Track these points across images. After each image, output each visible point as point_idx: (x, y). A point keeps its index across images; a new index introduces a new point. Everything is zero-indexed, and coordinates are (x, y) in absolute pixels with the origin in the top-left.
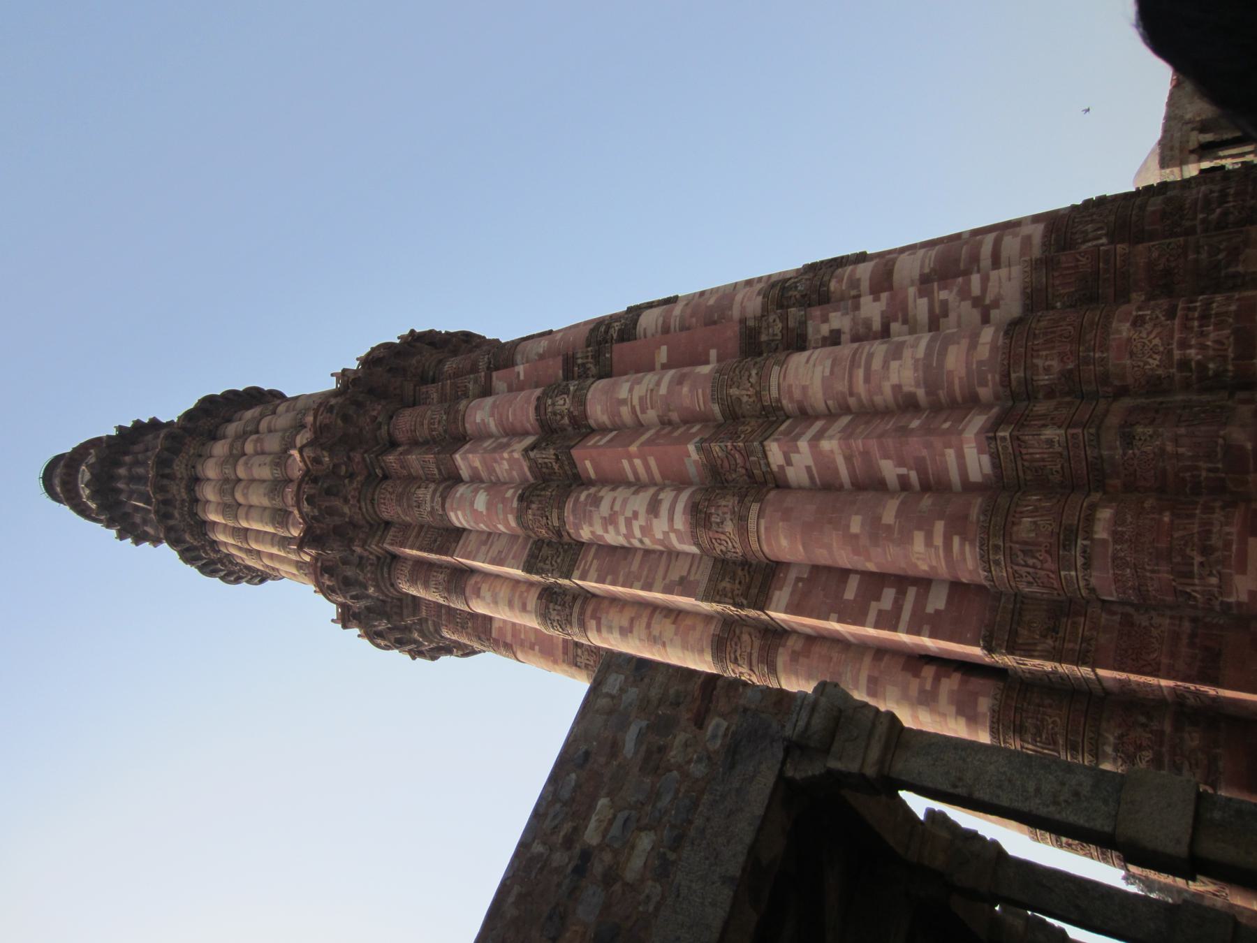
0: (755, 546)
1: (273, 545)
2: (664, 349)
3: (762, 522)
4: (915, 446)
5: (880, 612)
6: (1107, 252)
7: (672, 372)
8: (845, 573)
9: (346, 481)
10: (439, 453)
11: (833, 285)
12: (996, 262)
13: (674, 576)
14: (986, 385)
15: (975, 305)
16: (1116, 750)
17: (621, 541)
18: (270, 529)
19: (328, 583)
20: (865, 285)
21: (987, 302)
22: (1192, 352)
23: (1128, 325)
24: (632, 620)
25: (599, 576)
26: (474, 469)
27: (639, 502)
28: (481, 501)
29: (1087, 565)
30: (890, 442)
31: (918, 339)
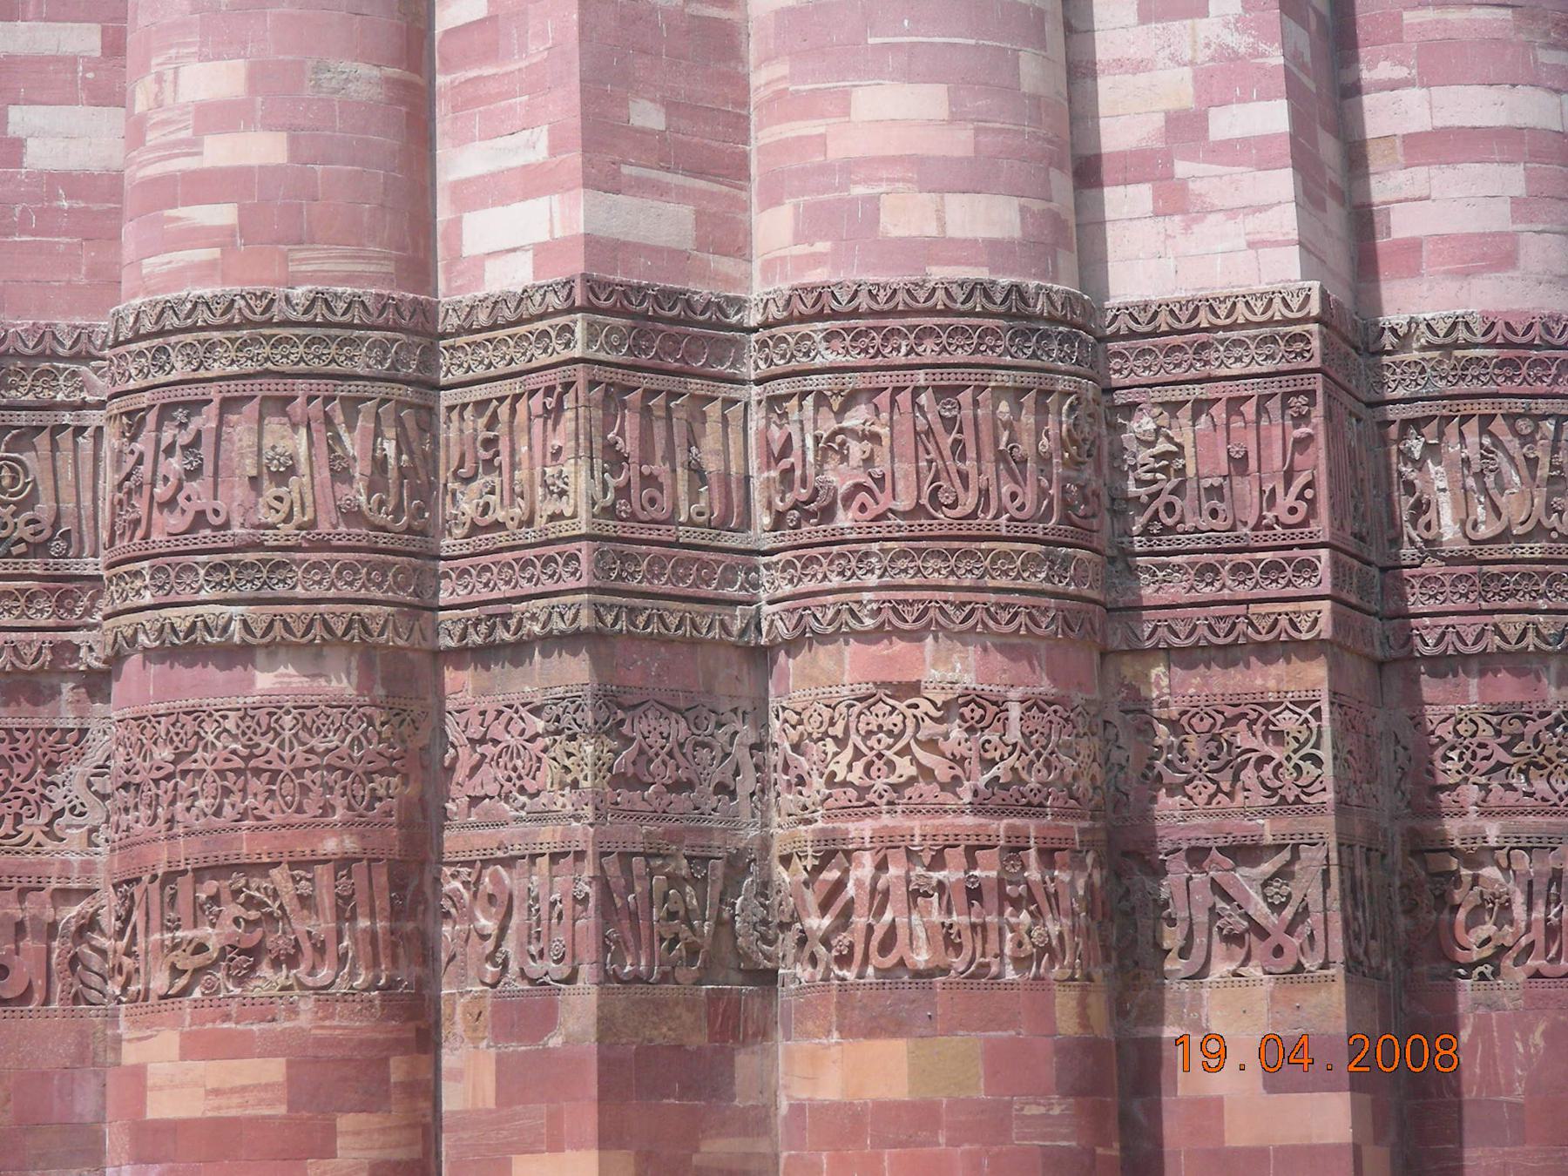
14: (799, 238)
21: (1182, 168)
22: (863, 870)
23: (969, 680)
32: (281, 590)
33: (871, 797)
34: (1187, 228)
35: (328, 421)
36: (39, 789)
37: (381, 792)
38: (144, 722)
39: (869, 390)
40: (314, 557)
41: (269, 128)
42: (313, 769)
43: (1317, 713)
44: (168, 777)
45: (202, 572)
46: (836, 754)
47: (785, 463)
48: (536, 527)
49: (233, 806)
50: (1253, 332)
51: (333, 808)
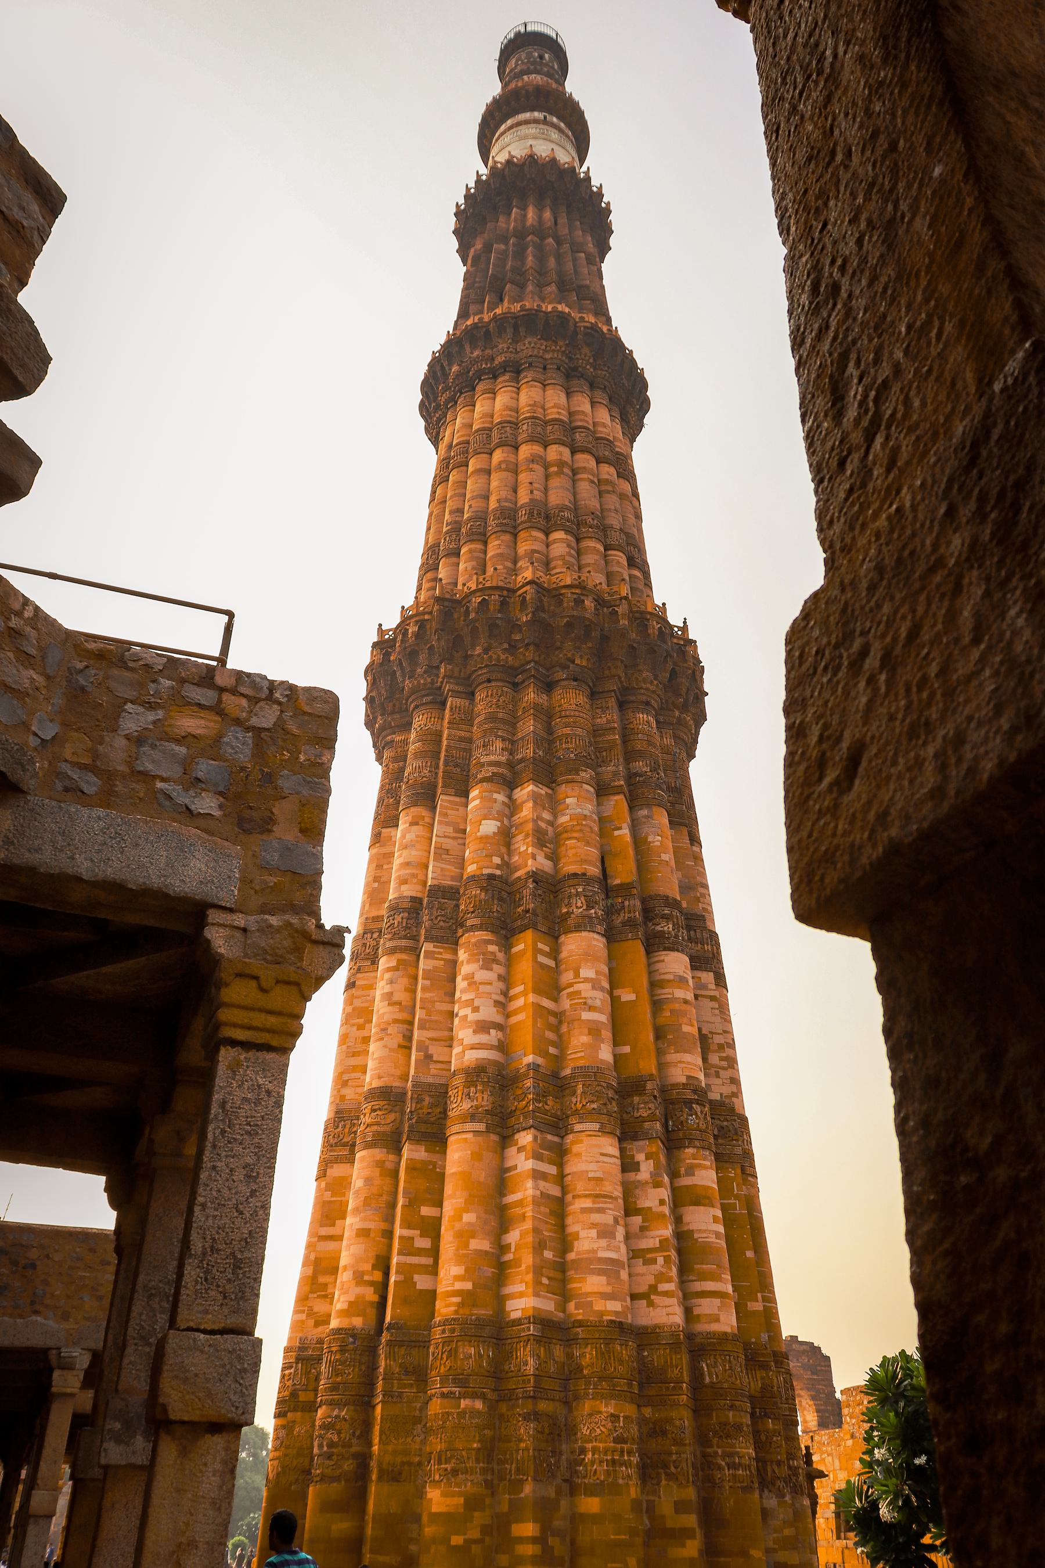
0: (455, 1128)
1: (451, 512)
2: (632, 997)
3: (470, 1136)
4: (528, 1260)
7: (603, 1018)
8: (440, 1205)
9: (506, 646)
13: (432, 1050)
14: (576, 1308)
15: (650, 1286)
16: (336, 1417)
17: (458, 995)
21: (652, 1297)
22: (590, 1456)
24: (400, 1003)
27: (488, 1012)
28: (489, 827)
29: (443, 1395)
30: (529, 1239)
31: (617, 1249)
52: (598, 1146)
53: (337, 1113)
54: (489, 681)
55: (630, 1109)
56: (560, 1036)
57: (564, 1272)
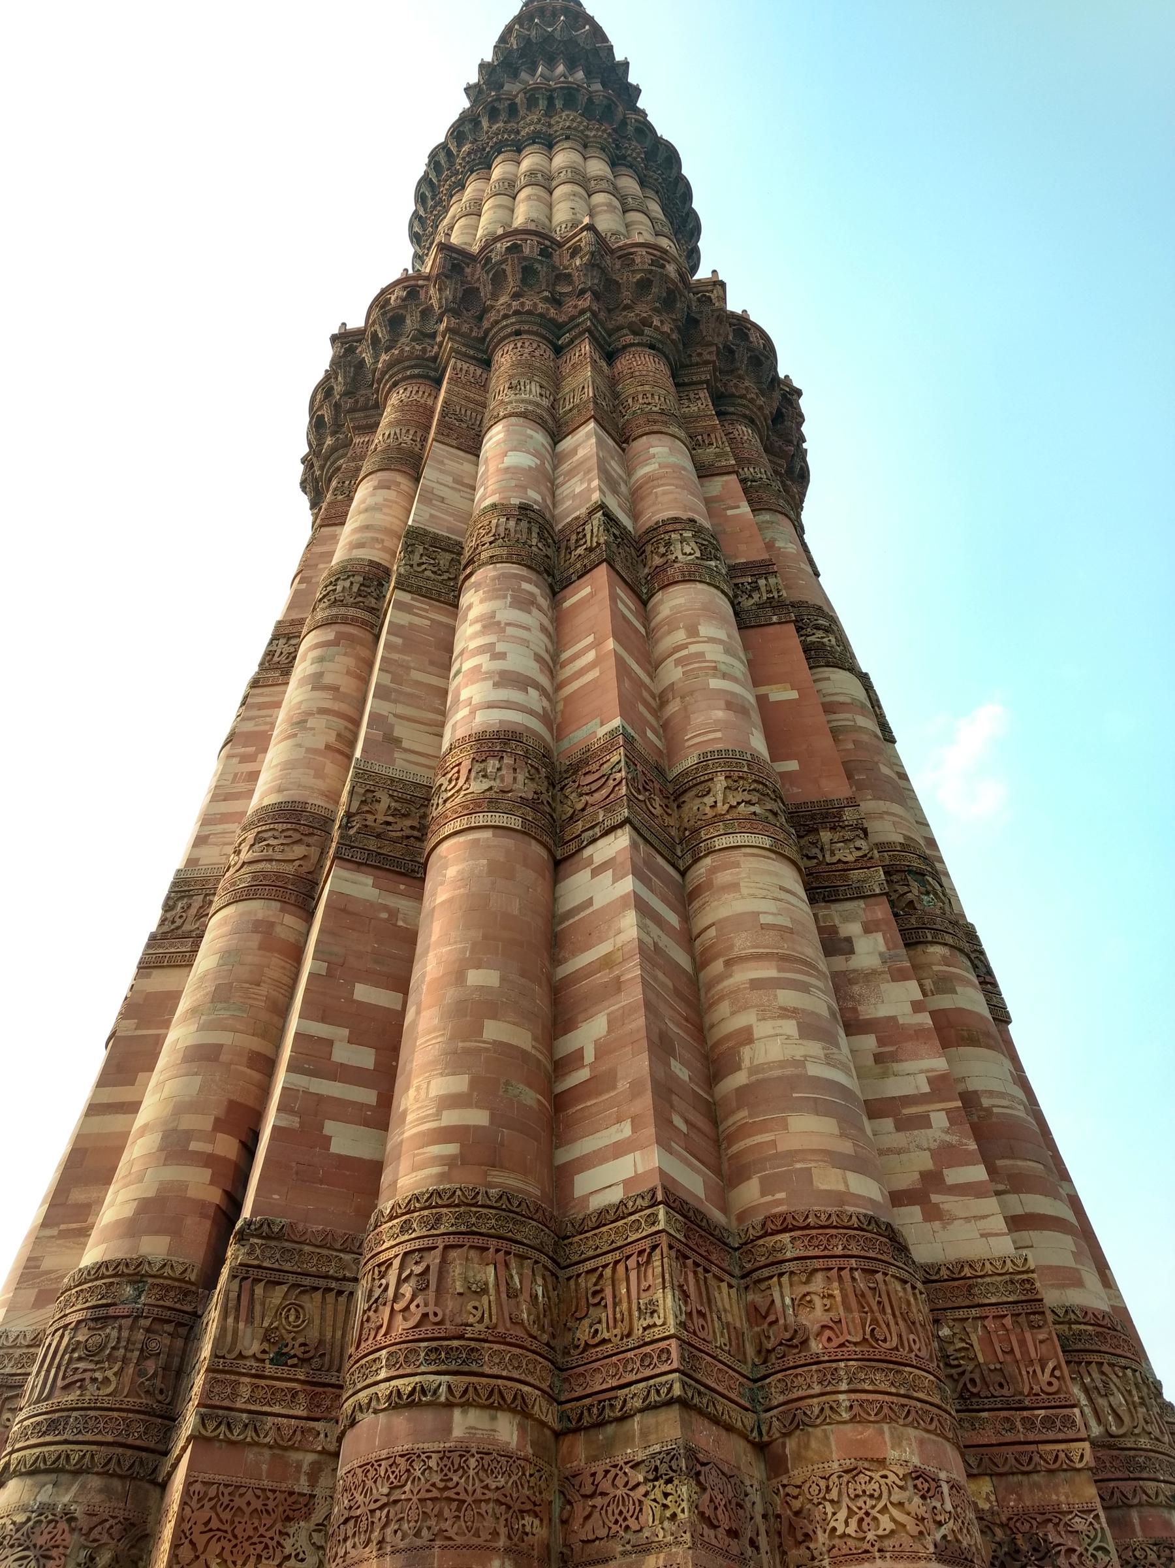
2: (794, 695)
3: (488, 834)
4: (636, 1065)
5: (330, 1043)
6: (1069, 1422)
7: (752, 700)
8: (402, 984)
10: (596, 403)
11: (937, 951)
12: (1017, 1223)
14: (763, 1194)
15: (925, 1176)
18: (480, 233)
19: (393, 297)
20: (944, 1002)
21: (935, 1198)
23: (916, 1460)
24: (335, 689)
25: (403, 626)
26: (574, 451)
27: (521, 662)
29: (399, 1403)
31: (846, 1070)
32: (474, 1367)
33: (866, 1546)
34: (944, 1228)
35: (507, 1265)
36: (277, 1538)
37: (528, 1529)
38: (369, 1467)
39: (822, 1270)
40: (496, 1347)
41: (478, 1107)
42: (487, 1501)
43: (1097, 1517)
44: (381, 1508)
45: (423, 1355)
46: (834, 1514)
47: (771, 1318)
48: (634, 1337)
49: (429, 1528)
50: (999, 1278)
51: (498, 1534)
52: (769, 873)
53: (174, 884)
54: (518, 333)
55: (817, 851)
56: (665, 726)
57: (715, 1122)
